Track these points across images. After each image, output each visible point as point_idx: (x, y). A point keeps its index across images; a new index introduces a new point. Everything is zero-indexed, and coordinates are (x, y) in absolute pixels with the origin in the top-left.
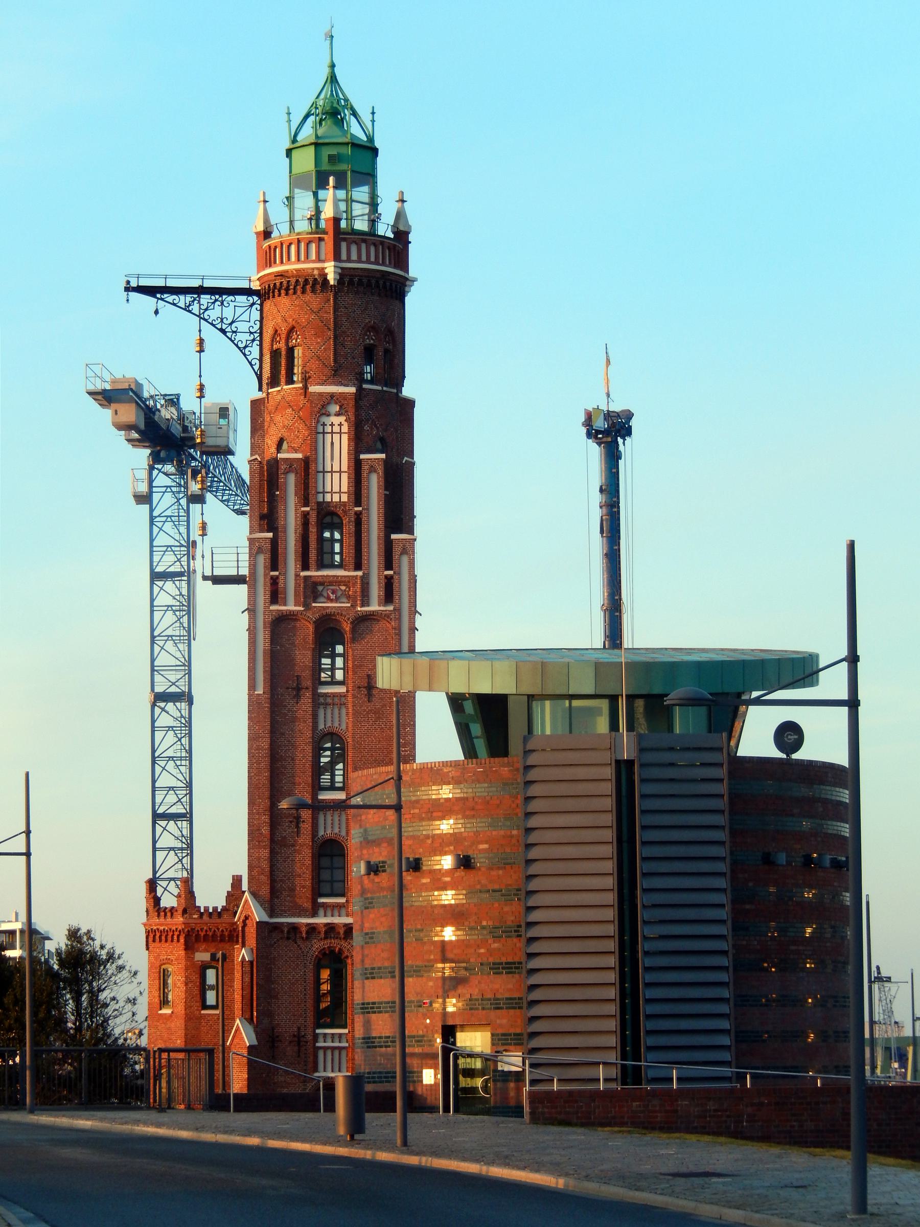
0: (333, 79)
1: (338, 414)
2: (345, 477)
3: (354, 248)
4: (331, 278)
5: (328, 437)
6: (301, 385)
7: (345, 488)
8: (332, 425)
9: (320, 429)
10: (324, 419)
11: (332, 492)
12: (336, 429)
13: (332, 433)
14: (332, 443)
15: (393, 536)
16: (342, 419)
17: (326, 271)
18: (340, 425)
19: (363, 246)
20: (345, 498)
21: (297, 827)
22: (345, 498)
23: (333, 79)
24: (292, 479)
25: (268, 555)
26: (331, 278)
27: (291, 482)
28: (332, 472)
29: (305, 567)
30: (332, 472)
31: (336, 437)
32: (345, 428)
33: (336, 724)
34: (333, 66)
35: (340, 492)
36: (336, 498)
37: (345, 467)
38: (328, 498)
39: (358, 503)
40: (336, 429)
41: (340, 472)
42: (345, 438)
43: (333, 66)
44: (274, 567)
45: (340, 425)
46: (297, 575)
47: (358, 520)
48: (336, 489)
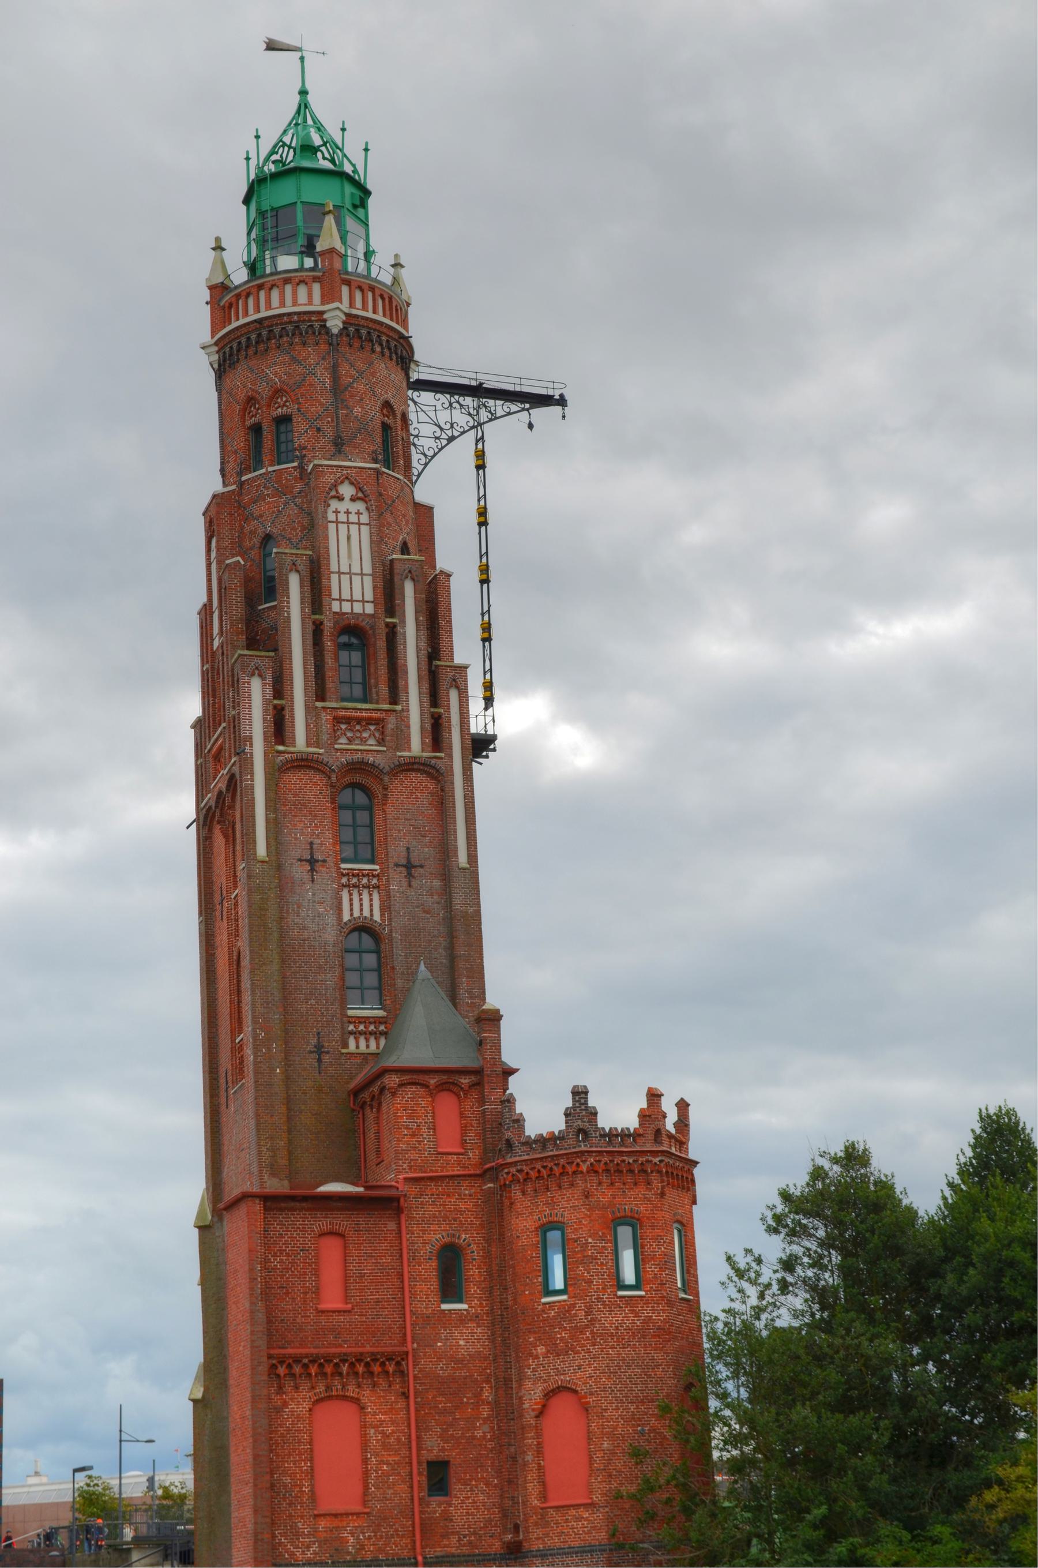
0: (303, 107)
1: (353, 499)
2: (368, 581)
3: (358, 295)
4: (335, 324)
5: (343, 528)
6: (295, 464)
7: (369, 596)
8: (348, 512)
9: (331, 517)
10: (334, 504)
11: (352, 601)
13: (348, 523)
14: (349, 538)
16: (360, 506)
17: (325, 316)
18: (358, 513)
19: (370, 295)
20: (369, 609)
21: (319, 1060)
22: (369, 609)
23: (303, 107)
26: (335, 324)
27: (294, 582)
28: (350, 573)
31: (354, 529)
32: (365, 518)
34: (303, 93)
36: (358, 608)
38: (346, 608)
40: (353, 518)
41: (362, 574)
42: (365, 529)
43: (303, 93)
45: (358, 513)
47: (392, 635)
48: (357, 595)
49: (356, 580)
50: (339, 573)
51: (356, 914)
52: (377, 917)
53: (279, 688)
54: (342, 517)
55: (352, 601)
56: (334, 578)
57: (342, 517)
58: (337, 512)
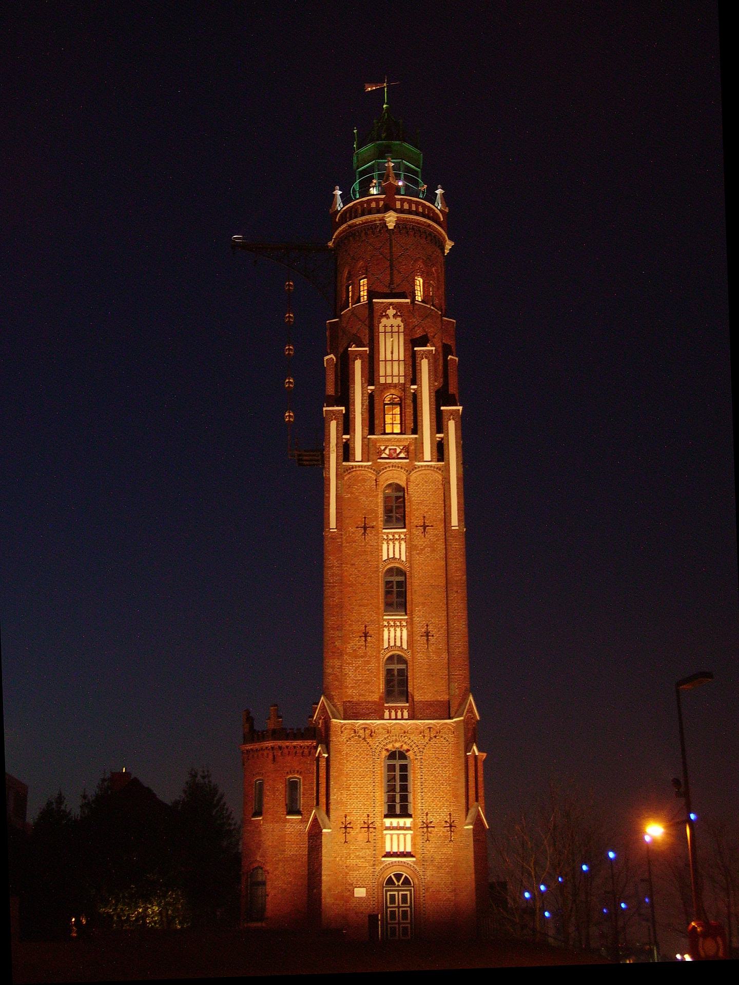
4: (391, 226)
7: (402, 373)
8: (392, 326)
9: (381, 329)
10: (384, 321)
11: (392, 376)
12: (395, 329)
15: (442, 408)
16: (399, 321)
21: (366, 640)
24: (358, 364)
25: (341, 422)
26: (391, 226)
28: (392, 361)
29: (372, 432)
30: (392, 361)
32: (402, 329)
33: (397, 556)
35: (399, 376)
36: (396, 381)
37: (402, 358)
39: (414, 382)
40: (395, 329)
41: (399, 360)
44: (346, 432)
45: (399, 326)
46: (363, 438)
49: (396, 364)
50: (386, 361)
51: (391, 556)
52: (403, 558)
53: (347, 426)
54: (389, 329)
55: (392, 376)
56: (382, 364)
57: (389, 329)
58: (385, 326)
